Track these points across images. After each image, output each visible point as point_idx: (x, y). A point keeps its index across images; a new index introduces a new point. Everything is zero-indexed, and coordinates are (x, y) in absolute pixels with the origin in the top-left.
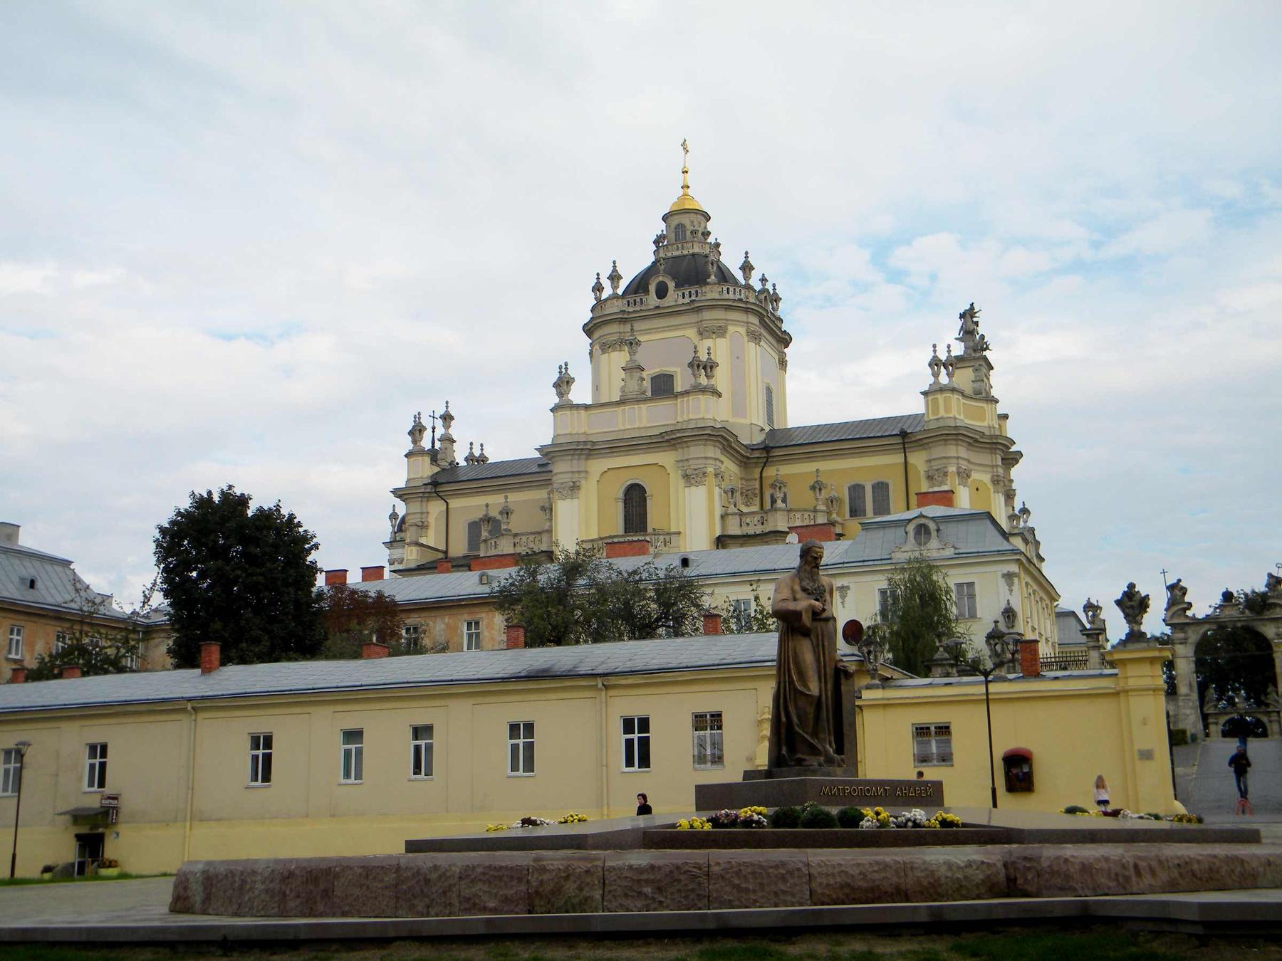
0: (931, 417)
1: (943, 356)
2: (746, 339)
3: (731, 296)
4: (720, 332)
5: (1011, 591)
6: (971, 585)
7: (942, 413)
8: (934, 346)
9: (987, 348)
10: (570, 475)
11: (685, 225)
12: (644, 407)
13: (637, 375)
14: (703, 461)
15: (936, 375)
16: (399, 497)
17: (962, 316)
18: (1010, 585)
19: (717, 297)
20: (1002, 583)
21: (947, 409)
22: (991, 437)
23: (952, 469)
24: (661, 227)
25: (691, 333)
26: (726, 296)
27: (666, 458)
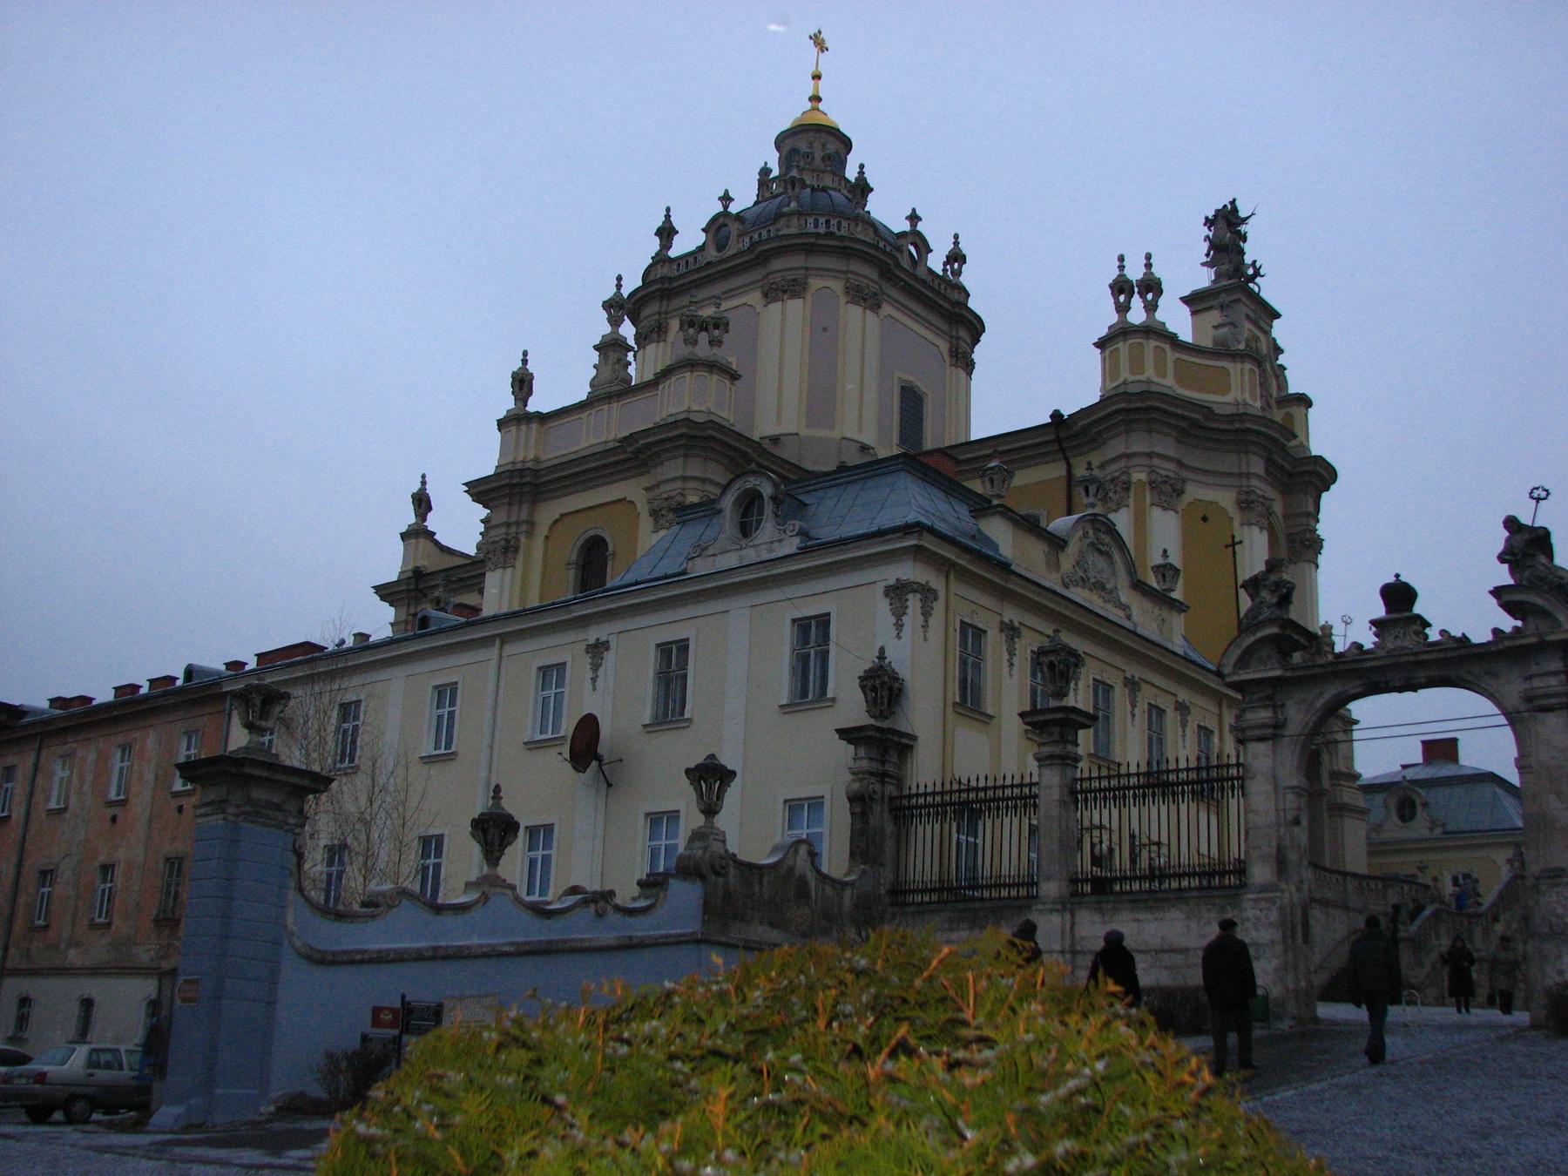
0: (1110, 385)
1: (1135, 273)
2: (843, 299)
3: (822, 230)
4: (795, 288)
5: (899, 627)
6: (824, 621)
7: (1125, 374)
8: (1121, 259)
9: (1257, 273)
10: (503, 530)
11: (814, 153)
12: (614, 405)
13: (613, 356)
14: (679, 484)
15: (1123, 309)
16: (383, 598)
17: (1209, 222)
18: (899, 613)
19: (796, 231)
20: (883, 607)
21: (1137, 364)
22: (1231, 418)
23: (1139, 476)
24: (773, 161)
25: (755, 298)
26: (811, 228)
27: (632, 489)
